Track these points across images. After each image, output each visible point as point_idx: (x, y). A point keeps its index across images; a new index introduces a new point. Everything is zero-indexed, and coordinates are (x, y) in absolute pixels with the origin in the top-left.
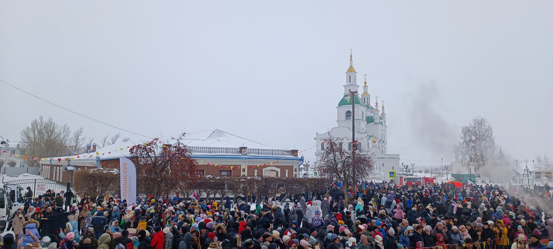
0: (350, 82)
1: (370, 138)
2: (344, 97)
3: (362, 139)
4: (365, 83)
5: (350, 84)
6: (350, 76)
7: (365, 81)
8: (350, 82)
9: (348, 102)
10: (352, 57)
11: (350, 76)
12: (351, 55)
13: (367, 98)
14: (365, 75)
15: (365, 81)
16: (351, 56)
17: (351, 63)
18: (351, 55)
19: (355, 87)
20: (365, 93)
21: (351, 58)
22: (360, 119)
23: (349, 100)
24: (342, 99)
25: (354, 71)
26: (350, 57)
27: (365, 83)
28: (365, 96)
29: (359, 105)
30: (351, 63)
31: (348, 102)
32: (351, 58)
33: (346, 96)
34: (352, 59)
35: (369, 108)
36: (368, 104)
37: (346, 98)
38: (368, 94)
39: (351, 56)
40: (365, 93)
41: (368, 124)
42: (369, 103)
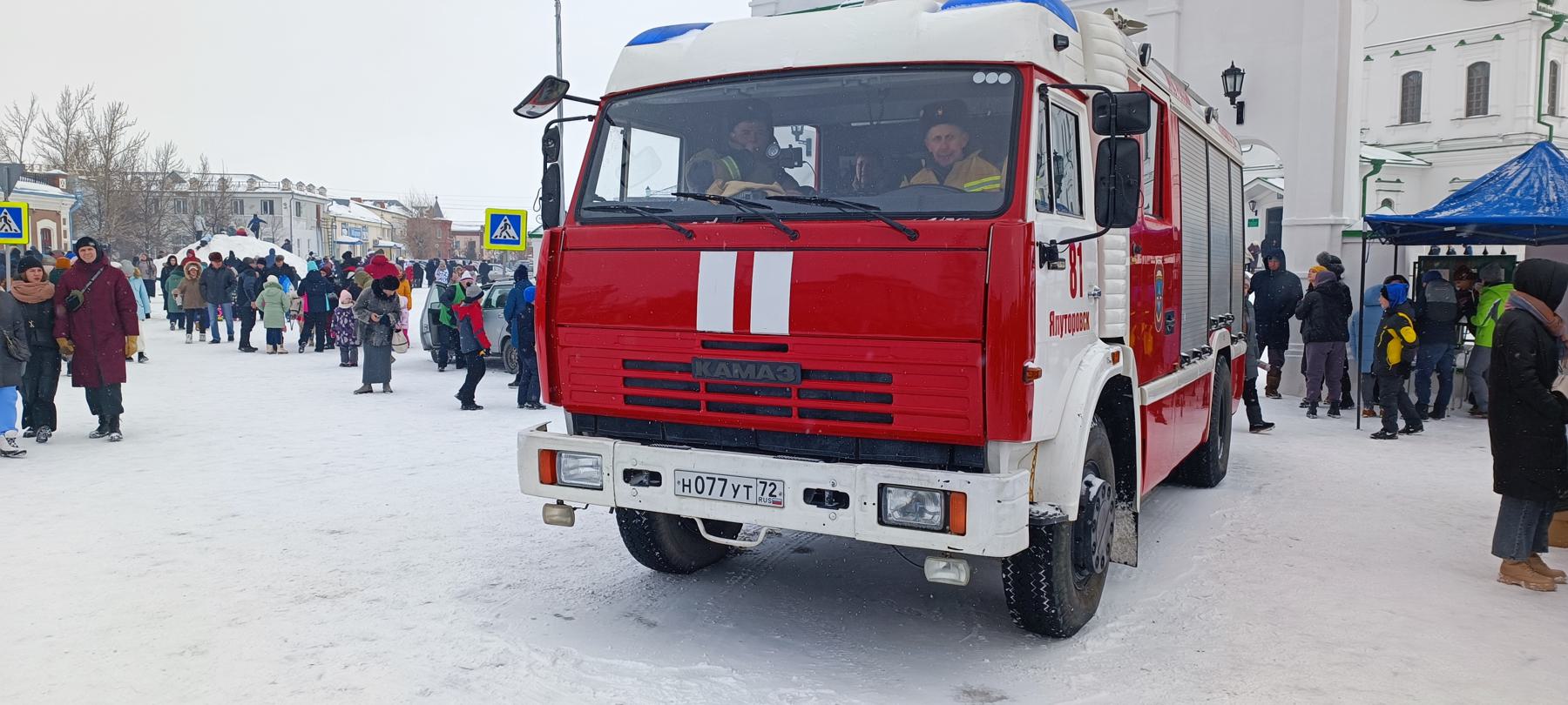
1: (1556, 27)
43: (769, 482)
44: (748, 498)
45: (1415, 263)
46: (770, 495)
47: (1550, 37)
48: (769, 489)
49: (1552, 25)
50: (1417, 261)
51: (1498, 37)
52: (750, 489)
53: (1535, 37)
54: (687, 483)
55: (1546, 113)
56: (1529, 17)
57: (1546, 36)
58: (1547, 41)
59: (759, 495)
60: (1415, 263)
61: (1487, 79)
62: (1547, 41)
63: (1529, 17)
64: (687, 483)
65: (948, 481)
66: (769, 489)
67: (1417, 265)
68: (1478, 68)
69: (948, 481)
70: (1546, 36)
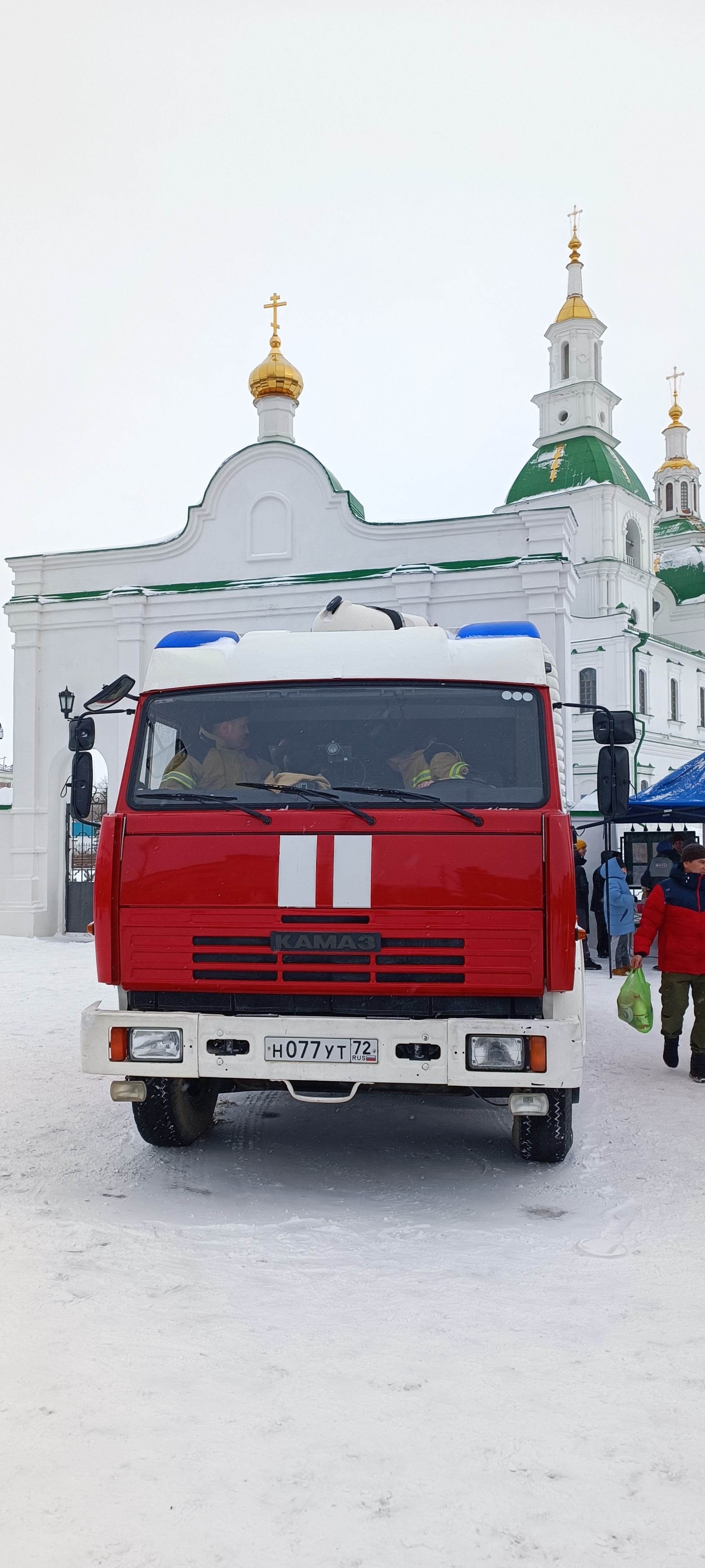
0: (566, 375)
1: (643, 643)
2: (534, 457)
3: (601, 649)
4: (675, 414)
5: (568, 382)
6: (566, 348)
7: (676, 405)
8: (566, 375)
9: (553, 475)
10: (578, 251)
11: (566, 348)
12: (575, 237)
13: (684, 485)
14: (675, 376)
15: (676, 405)
16: (574, 245)
17: (575, 280)
18: (575, 237)
19: (588, 396)
20: (671, 459)
21: (575, 254)
22: (609, 554)
23: (555, 464)
24: (528, 466)
25: (590, 318)
26: (571, 251)
27: (675, 414)
28: (670, 472)
29: (607, 482)
30: (575, 280)
31: (553, 475)
32: (575, 254)
33: (546, 449)
34: (580, 259)
35: (689, 527)
36: (688, 511)
37: (544, 457)
38: (689, 466)
39: (574, 245)
40: (676, 461)
41: (678, 604)
42: (691, 506)
43: (363, 1041)
44: (342, 1058)
45: (621, 838)
46: (365, 1053)
47: (638, 651)
48: (363, 1048)
49: (639, 641)
50: (623, 836)
51: (601, 649)
52: (343, 1049)
53: (627, 649)
54: (277, 1048)
55: (639, 712)
56: (623, 633)
57: (635, 650)
58: (636, 653)
59: (353, 1054)
60: (621, 838)
61: (595, 682)
62: (636, 653)
63: (623, 633)
64: (277, 1048)
65: (530, 1028)
66: (363, 1048)
67: (623, 840)
68: (587, 673)
69: (530, 1028)
70: (635, 650)
